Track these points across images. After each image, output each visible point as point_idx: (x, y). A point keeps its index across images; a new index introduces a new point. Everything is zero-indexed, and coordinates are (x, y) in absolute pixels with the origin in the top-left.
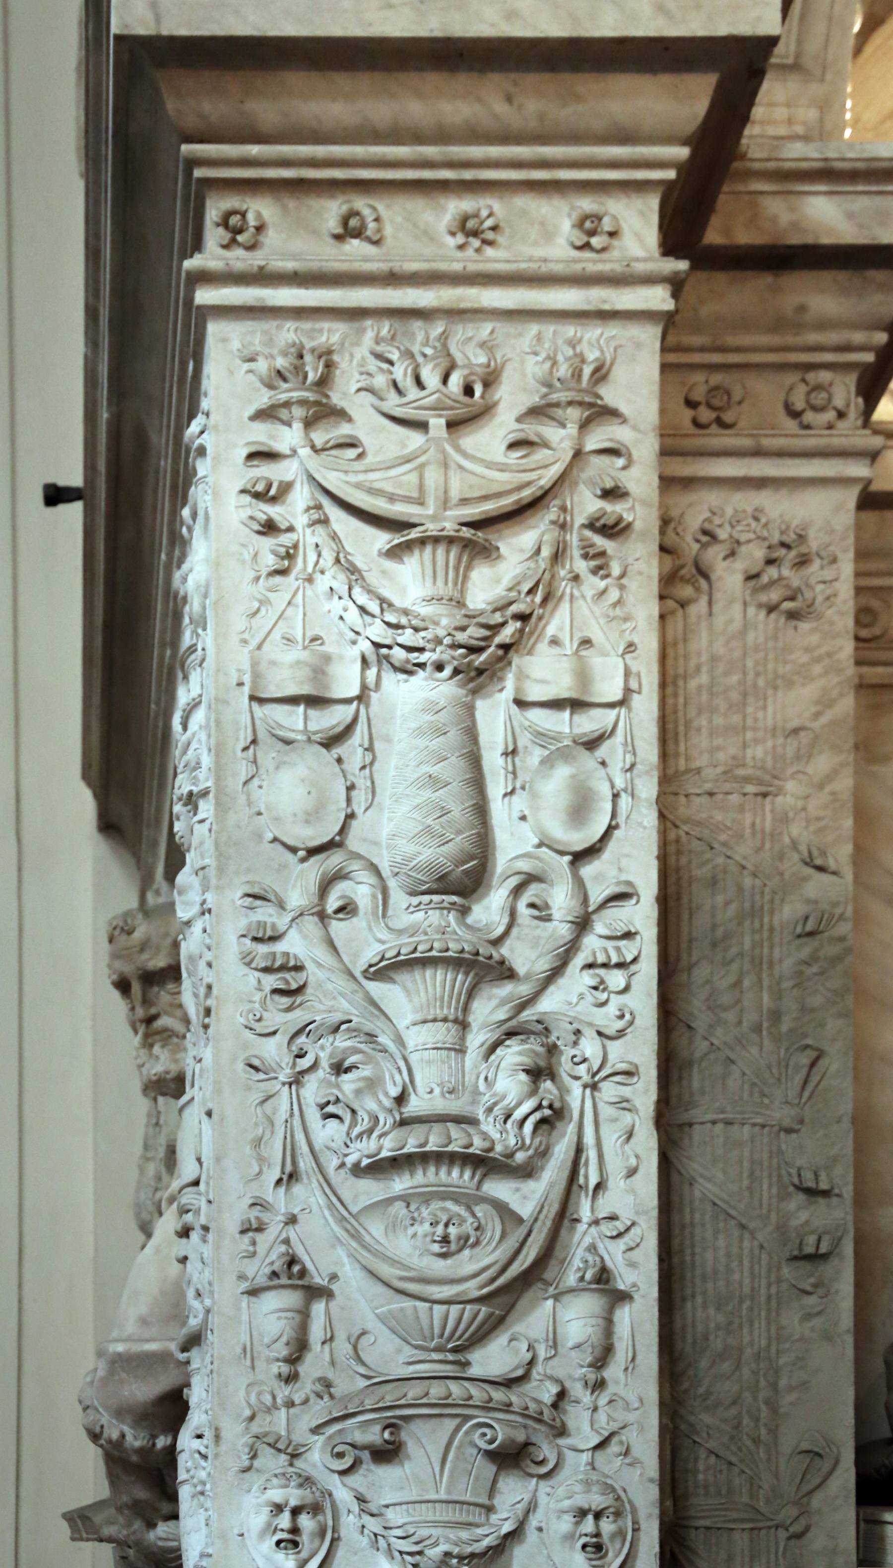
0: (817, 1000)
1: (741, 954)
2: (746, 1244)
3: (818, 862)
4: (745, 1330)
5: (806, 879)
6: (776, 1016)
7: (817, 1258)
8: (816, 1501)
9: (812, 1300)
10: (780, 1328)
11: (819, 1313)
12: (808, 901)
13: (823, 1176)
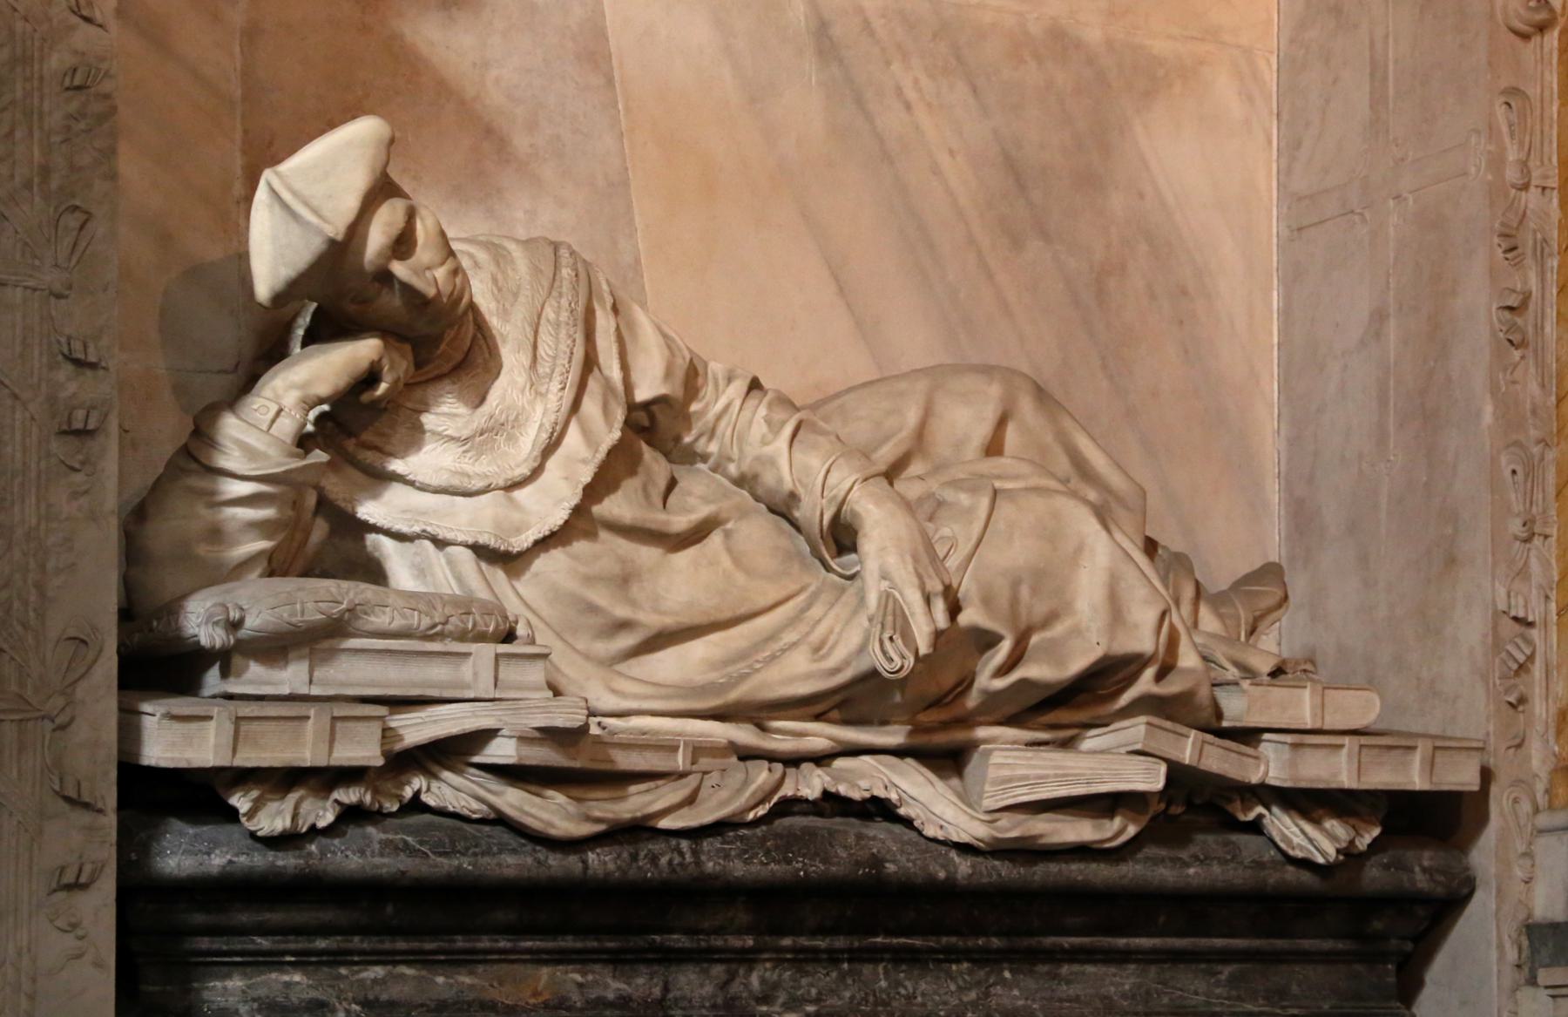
0: (85, 159)
1: (13, 102)
2: (18, 415)
3: (85, 13)
4: (17, 509)
5: (72, 28)
6: (45, 171)
7: (84, 433)
8: (80, 691)
9: (78, 478)
10: (49, 506)
11: (86, 492)
12: (76, 52)
13: (91, 350)
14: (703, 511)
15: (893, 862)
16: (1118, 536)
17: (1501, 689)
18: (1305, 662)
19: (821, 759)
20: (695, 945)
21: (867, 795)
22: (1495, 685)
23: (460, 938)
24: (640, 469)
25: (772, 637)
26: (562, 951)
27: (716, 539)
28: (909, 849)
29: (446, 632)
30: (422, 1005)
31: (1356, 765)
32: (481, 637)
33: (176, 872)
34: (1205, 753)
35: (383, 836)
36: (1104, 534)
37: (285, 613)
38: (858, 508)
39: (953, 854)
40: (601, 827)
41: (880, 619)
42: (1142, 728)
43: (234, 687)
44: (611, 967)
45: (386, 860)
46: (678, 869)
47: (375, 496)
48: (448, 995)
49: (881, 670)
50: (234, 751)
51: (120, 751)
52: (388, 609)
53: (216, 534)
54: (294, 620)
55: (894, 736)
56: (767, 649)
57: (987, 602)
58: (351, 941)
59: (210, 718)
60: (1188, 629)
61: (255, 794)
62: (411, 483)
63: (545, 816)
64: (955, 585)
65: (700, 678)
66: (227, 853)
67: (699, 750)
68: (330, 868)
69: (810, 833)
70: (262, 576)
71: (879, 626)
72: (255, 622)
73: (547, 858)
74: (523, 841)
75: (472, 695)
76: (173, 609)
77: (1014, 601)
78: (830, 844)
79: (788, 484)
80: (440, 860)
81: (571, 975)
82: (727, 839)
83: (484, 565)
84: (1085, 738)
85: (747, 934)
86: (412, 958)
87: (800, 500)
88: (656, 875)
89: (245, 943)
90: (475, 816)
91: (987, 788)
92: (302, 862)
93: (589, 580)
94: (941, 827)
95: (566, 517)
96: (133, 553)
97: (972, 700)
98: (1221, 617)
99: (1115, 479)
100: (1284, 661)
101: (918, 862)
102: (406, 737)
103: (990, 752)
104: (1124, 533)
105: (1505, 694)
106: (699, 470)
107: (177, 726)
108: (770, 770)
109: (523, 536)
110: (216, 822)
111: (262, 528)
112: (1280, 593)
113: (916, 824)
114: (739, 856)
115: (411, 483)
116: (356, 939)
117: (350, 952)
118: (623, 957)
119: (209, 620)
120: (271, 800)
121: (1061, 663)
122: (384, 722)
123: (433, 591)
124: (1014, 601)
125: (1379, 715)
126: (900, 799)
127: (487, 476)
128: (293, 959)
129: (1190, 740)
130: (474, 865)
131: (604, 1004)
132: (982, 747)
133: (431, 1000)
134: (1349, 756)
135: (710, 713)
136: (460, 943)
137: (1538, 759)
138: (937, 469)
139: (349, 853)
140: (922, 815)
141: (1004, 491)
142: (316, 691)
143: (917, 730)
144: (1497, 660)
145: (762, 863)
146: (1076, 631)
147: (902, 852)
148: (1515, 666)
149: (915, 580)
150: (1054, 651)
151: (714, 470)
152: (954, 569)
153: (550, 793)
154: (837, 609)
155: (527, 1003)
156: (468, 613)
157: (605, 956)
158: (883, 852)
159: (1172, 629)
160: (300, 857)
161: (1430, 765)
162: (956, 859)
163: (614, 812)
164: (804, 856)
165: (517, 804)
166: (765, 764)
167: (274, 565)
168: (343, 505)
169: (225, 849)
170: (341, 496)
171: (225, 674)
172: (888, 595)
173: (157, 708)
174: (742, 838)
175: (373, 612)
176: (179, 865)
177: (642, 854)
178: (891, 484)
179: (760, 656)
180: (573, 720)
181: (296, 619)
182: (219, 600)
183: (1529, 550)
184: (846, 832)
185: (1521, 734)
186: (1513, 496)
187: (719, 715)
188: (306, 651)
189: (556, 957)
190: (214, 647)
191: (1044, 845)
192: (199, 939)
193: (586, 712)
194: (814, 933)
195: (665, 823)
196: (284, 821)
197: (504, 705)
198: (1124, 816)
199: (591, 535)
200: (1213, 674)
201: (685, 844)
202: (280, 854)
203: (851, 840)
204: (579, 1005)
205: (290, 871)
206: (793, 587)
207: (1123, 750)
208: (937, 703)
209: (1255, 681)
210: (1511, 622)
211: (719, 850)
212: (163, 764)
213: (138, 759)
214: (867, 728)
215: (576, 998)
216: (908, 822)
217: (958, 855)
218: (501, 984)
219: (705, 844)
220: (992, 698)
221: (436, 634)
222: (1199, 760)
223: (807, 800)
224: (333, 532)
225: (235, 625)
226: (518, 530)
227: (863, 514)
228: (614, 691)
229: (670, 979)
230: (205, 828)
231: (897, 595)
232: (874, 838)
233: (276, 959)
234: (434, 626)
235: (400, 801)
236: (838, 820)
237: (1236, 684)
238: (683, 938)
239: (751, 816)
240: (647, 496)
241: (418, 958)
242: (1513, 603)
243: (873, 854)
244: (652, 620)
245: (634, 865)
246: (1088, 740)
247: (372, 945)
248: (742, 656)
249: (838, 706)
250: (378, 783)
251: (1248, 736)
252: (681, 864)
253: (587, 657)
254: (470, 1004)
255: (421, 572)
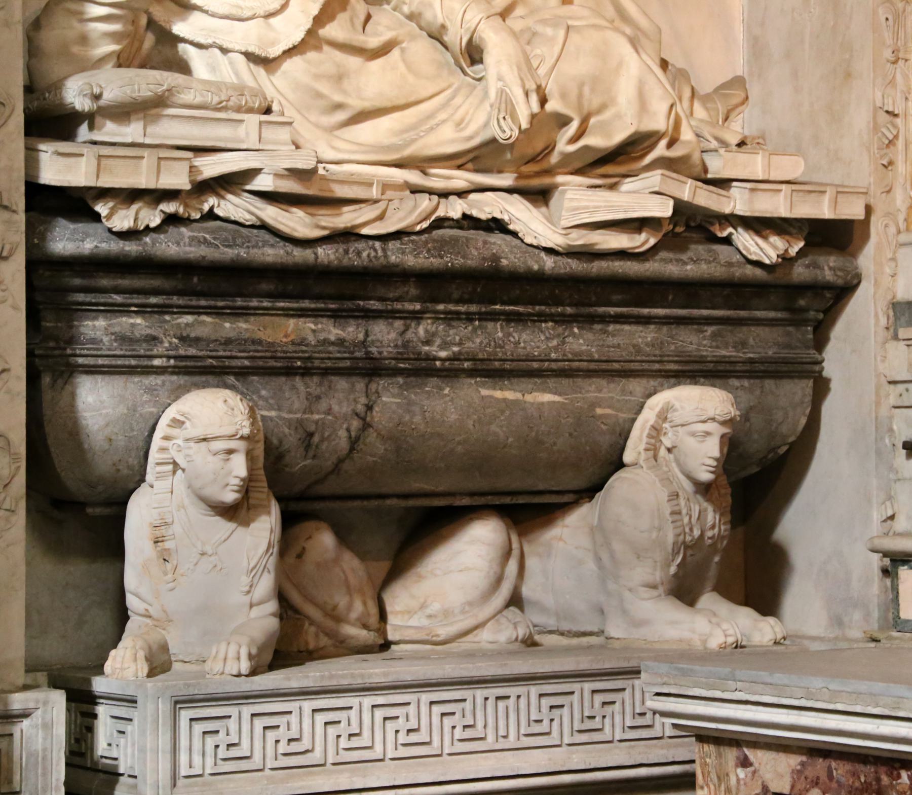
14: (387, 36)
15: (506, 258)
16: (644, 57)
17: (878, 156)
18: (759, 138)
19: (461, 194)
20: (384, 308)
21: (490, 217)
22: (874, 153)
23: (239, 299)
24: (349, 8)
25: (431, 116)
26: (302, 309)
27: (395, 53)
28: (515, 250)
29: (229, 106)
30: (216, 340)
31: (789, 203)
32: (250, 110)
33: (62, 252)
34: (697, 194)
35: (191, 234)
36: (635, 54)
37: (128, 91)
38: (483, 35)
39: (543, 254)
40: (325, 233)
41: (497, 105)
42: (659, 177)
43: (97, 136)
44: (333, 320)
45: (193, 249)
46: (373, 260)
47: (184, 20)
48: (232, 335)
49: (498, 138)
50: (98, 177)
51: (26, 174)
52: (192, 91)
53: (84, 40)
54: (134, 95)
55: (506, 180)
56: (427, 124)
57: (564, 96)
58: (172, 299)
59: (82, 155)
60: (687, 117)
61: (111, 204)
62: (206, 12)
63: (291, 224)
64: (543, 85)
65: (386, 141)
66: (94, 241)
67: (386, 186)
68: (159, 253)
69: (455, 240)
70: (114, 67)
71: (497, 110)
72: (110, 95)
73: (292, 250)
74: (278, 240)
75: (245, 147)
76: (58, 86)
77: (580, 96)
78: (467, 246)
79: (440, 20)
80: (226, 249)
81: (308, 325)
82: (405, 242)
83: (252, 65)
84: (623, 184)
85: (416, 302)
86: (209, 311)
87: (447, 30)
88: (360, 263)
89: (106, 298)
90: (248, 223)
91: (564, 213)
92: (141, 248)
93: (317, 77)
94: (535, 237)
95: (303, 36)
96: (33, 50)
97: (554, 159)
98: (707, 109)
99: (643, 22)
100: (746, 137)
101: (522, 259)
102: (204, 172)
103: (565, 191)
104: (648, 55)
105: (881, 159)
106: (384, 9)
107: (61, 159)
108: (430, 199)
109: (276, 48)
110: (87, 222)
111: (114, 37)
112: (743, 95)
113: (520, 235)
114: (411, 253)
115: (206, 12)
116: (175, 298)
117: (171, 306)
118: (340, 314)
119: (81, 93)
120: (121, 209)
121: (609, 136)
122: (191, 162)
123: (220, 80)
124: (580, 96)
125: (803, 173)
126: (510, 220)
127: (253, 8)
128: (136, 309)
129: (688, 185)
130: (248, 254)
131: (329, 343)
132: (560, 188)
133: (222, 337)
134: (785, 197)
135: (394, 163)
136: (239, 302)
137: (900, 200)
138: (533, 12)
139: (170, 244)
140: (523, 229)
141: (574, 27)
142: (148, 141)
143: (521, 176)
144: (876, 138)
145: (425, 258)
146: (618, 116)
147: (511, 252)
148: (887, 142)
149: (519, 82)
150: (604, 128)
151: (395, 9)
152: (543, 74)
153: (294, 210)
154: (470, 99)
155: (281, 341)
156: (243, 95)
157: (329, 313)
158: (499, 251)
159: (677, 115)
160: (139, 245)
161: (835, 203)
162: (544, 257)
163: (333, 223)
164: (451, 253)
165: (274, 216)
166: (427, 195)
167: (121, 61)
168: (163, 24)
169: (92, 239)
170: (162, 19)
171: (91, 128)
172: (502, 91)
173: (49, 148)
174: (413, 242)
175: (183, 92)
176: (64, 247)
177: (351, 250)
178: (504, 20)
179: (424, 128)
180: (309, 164)
181: (135, 95)
182: (86, 81)
183: (896, 68)
184: (477, 240)
185: (890, 184)
186: (886, 35)
187: (399, 164)
188: (141, 115)
189: (299, 313)
190: (84, 111)
191: (599, 249)
192: (78, 294)
193: (316, 159)
194: (459, 301)
195: (365, 231)
196: (129, 221)
197: (264, 153)
198: (647, 232)
199: (318, 48)
200: (702, 145)
201: (377, 244)
202: (127, 243)
203: (480, 244)
204: (313, 343)
205: (134, 254)
206: (444, 85)
207: (647, 191)
208: (533, 160)
209: (728, 149)
210: (885, 114)
211: (399, 249)
212: (53, 183)
213: (37, 179)
214: (490, 175)
215: (311, 339)
216: (515, 234)
217: (546, 255)
218: (265, 328)
219: (390, 245)
220: (567, 158)
221: (222, 107)
222: (693, 198)
223: (453, 219)
224: (158, 42)
225: (97, 97)
226: (273, 44)
227: (487, 39)
228: (333, 148)
229: (369, 329)
230: (80, 225)
231: (508, 91)
232: (494, 243)
233: (126, 309)
234: (221, 102)
235: (201, 212)
236: (472, 232)
237: (716, 151)
238: (377, 303)
239: (418, 228)
240: (353, 24)
241: (213, 311)
242: (886, 101)
243: (494, 253)
244: (357, 104)
245: (346, 257)
246: (625, 185)
247: (184, 302)
248: (413, 127)
249: (471, 161)
250: (187, 201)
251: (723, 183)
252: (376, 257)
253: (317, 126)
254: (246, 341)
255: (213, 69)
